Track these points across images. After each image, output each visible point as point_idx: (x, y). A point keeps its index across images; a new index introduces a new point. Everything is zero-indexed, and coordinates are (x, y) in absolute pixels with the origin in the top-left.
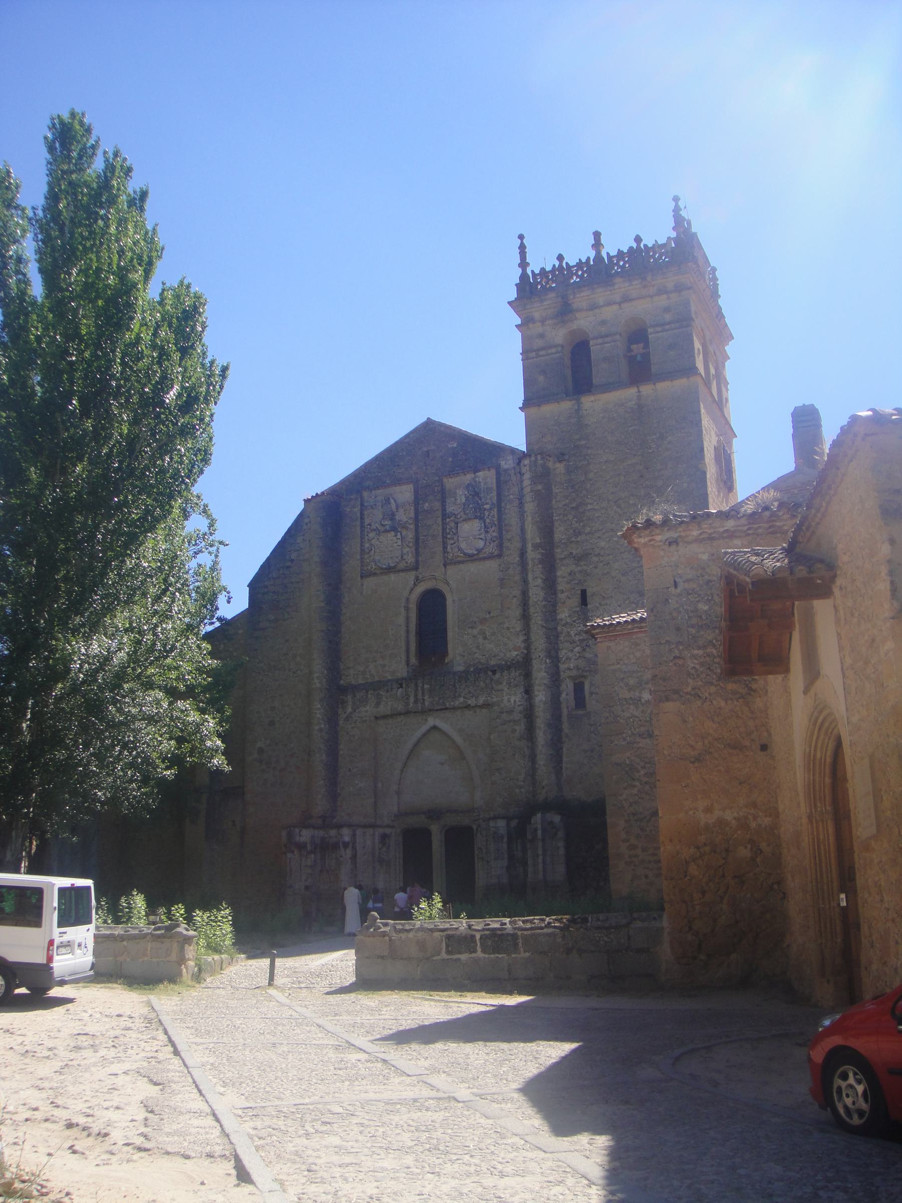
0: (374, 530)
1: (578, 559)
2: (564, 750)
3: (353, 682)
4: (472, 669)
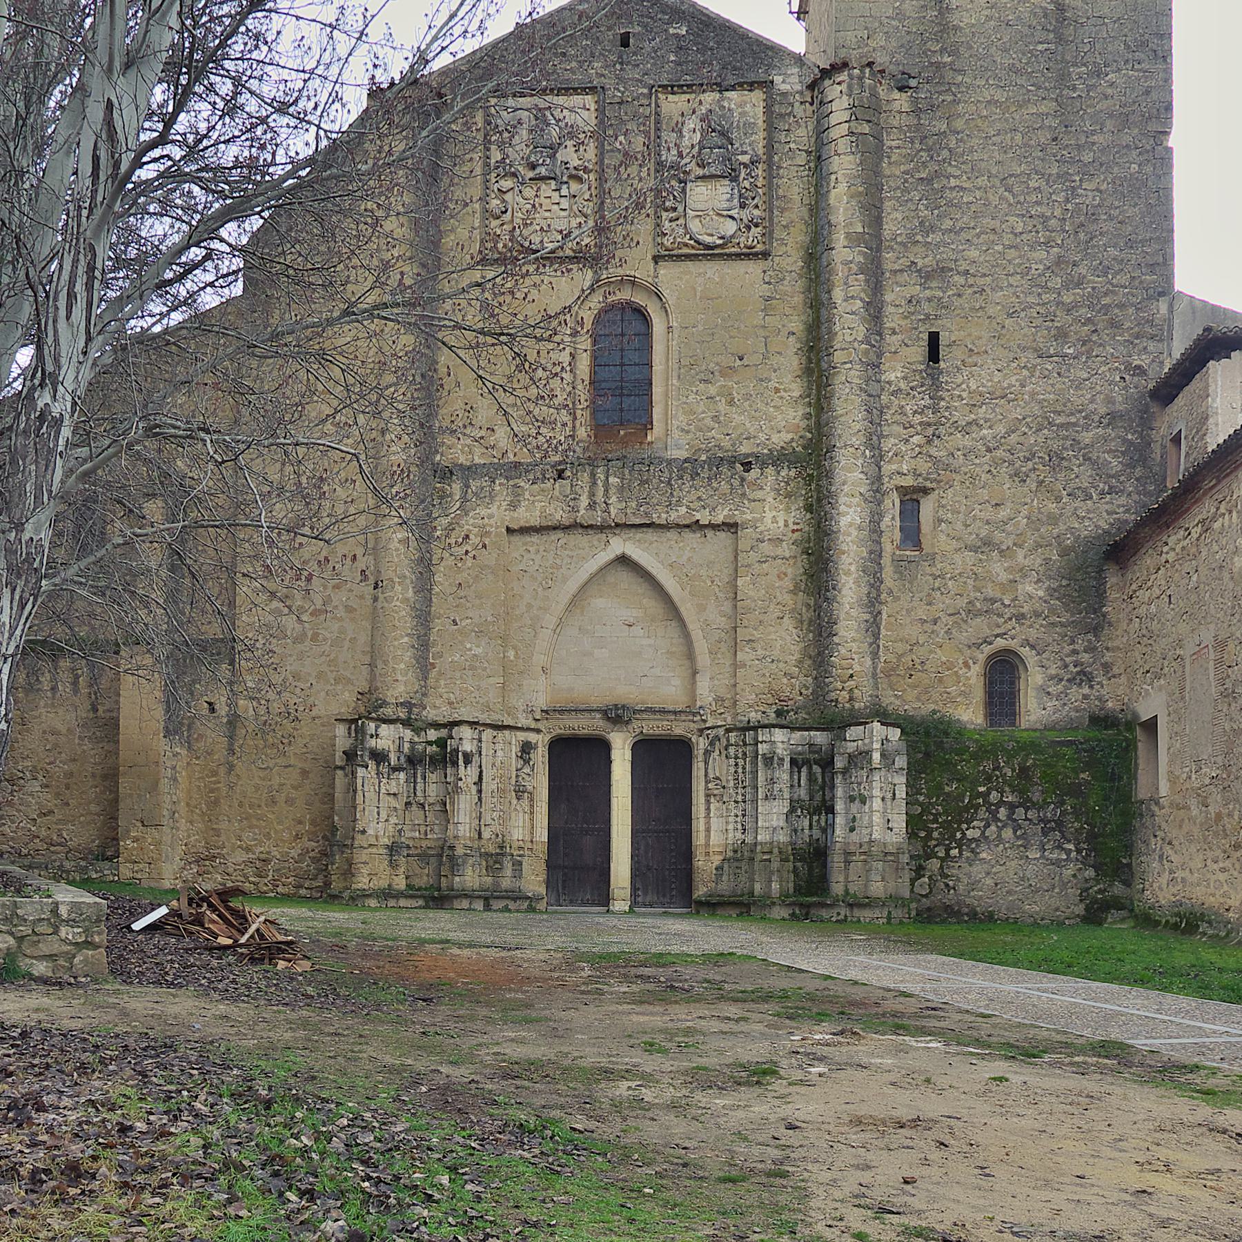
0: (514, 175)
1: (926, 276)
2: (884, 616)
3: (462, 460)
4: (704, 458)
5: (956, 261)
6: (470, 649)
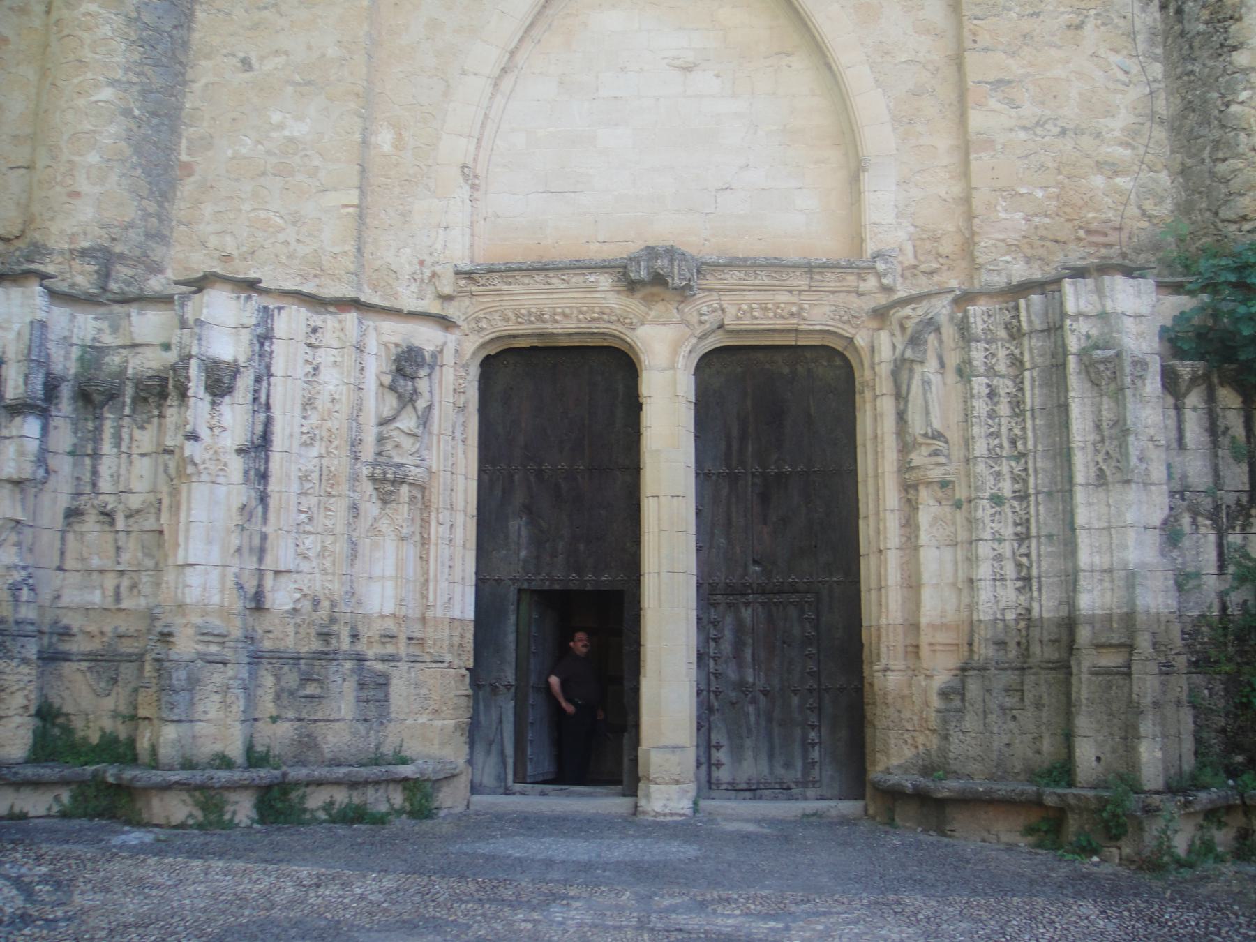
6: (281, 127)
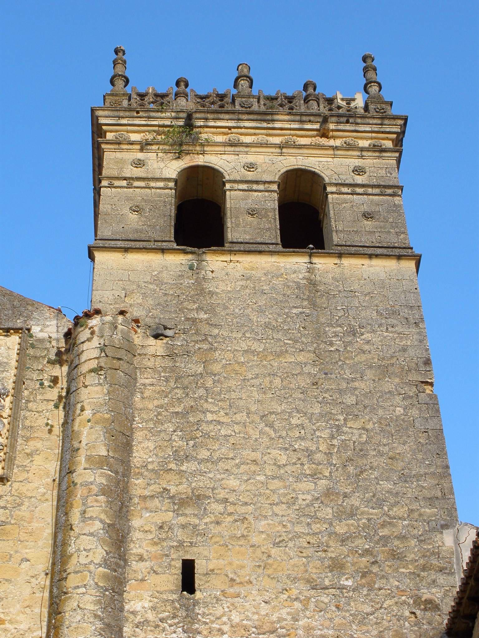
5: (213, 489)
